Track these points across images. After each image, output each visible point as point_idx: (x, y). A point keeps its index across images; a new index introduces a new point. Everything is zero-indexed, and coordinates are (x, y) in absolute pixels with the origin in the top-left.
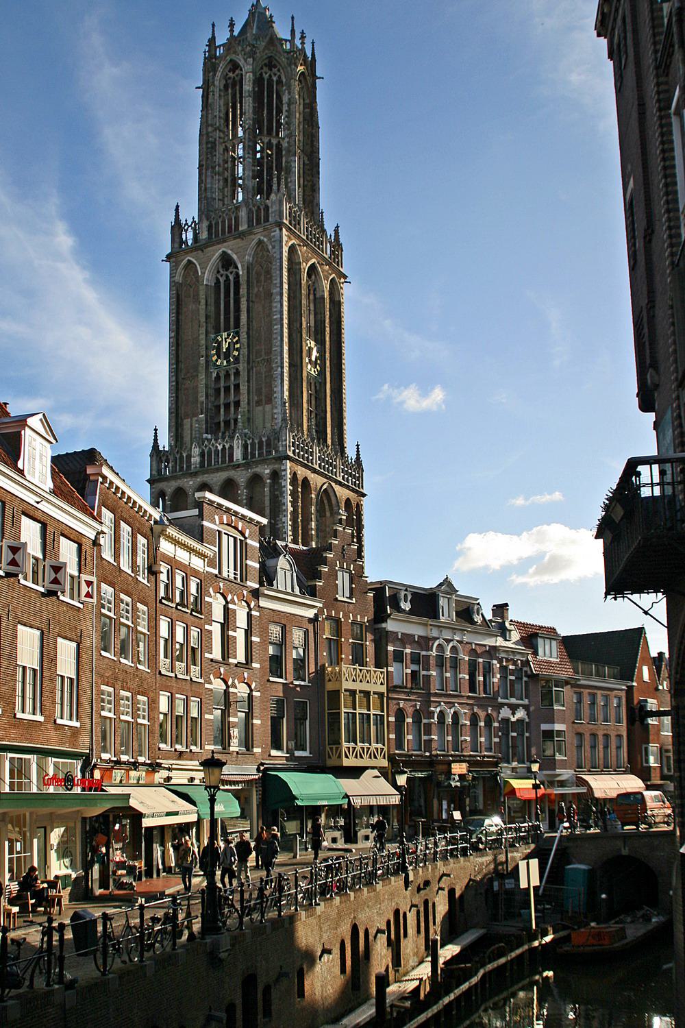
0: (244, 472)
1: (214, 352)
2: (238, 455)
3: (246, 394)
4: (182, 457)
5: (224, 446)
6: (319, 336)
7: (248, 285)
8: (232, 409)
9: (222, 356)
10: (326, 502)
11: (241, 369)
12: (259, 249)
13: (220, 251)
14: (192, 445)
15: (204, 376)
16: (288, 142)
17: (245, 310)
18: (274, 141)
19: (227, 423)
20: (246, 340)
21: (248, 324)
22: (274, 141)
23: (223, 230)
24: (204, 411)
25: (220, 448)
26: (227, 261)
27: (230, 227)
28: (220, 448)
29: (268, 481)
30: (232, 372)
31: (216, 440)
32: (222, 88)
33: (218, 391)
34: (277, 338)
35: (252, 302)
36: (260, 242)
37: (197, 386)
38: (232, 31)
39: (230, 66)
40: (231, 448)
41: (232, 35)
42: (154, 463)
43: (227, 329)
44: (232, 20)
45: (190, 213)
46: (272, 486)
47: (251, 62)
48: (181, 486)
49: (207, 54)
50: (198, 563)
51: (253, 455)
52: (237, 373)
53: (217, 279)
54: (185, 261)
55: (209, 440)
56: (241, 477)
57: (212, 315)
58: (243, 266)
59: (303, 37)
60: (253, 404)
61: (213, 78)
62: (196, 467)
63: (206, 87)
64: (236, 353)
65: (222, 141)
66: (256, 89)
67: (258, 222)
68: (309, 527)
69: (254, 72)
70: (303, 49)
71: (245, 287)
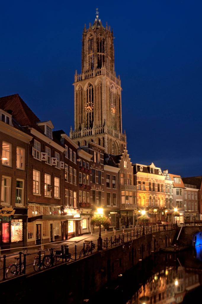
2: (93, 133)
13: (88, 83)
28: (89, 131)
29: (102, 140)
40: (91, 132)
58: (94, 86)
71: (95, 91)
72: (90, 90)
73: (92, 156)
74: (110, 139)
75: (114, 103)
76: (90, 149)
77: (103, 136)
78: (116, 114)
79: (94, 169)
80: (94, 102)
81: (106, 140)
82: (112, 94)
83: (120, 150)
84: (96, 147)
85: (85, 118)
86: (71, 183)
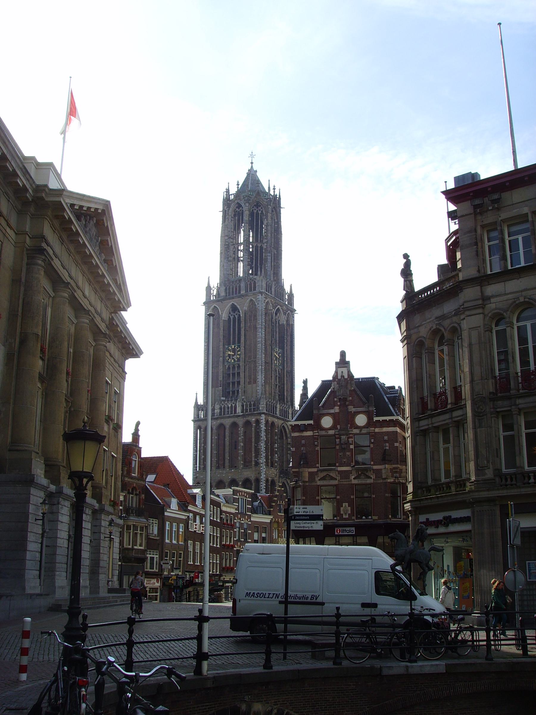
0: (242, 419)
2: (239, 410)
3: (243, 379)
5: (232, 405)
7: (245, 322)
8: (236, 385)
10: (283, 432)
11: (241, 365)
12: (251, 303)
13: (231, 303)
14: (215, 403)
15: (222, 367)
16: (266, 246)
17: (243, 335)
18: (259, 245)
19: (233, 392)
20: (244, 351)
21: (245, 343)
22: (259, 245)
24: (222, 385)
25: (230, 406)
26: (234, 308)
27: (236, 289)
28: (230, 406)
29: (254, 424)
30: (236, 366)
31: (228, 401)
32: (233, 216)
33: (229, 375)
34: (259, 351)
35: (247, 331)
36: (251, 300)
37: (218, 372)
38: (238, 187)
41: (238, 190)
42: (195, 411)
44: (238, 182)
45: (215, 282)
46: (256, 427)
47: (248, 205)
49: (225, 196)
50: (233, 511)
51: (247, 410)
52: (239, 367)
53: (229, 317)
54: (213, 306)
55: (224, 401)
56: (241, 422)
59: (274, 189)
60: (247, 383)
61: (228, 211)
62: (217, 415)
63: (225, 213)
65: (232, 243)
66: (250, 219)
67: (251, 290)
68: (275, 447)
69: (249, 211)
70: (274, 193)
71: (243, 323)
72: (234, 317)
73: (238, 504)
74: (270, 423)
76: (234, 496)
79: (239, 521)
80: (242, 344)
81: (263, 427)
82: (277, 325)
83: (290, 444)
84: (242, 492)
86: (215, 546)
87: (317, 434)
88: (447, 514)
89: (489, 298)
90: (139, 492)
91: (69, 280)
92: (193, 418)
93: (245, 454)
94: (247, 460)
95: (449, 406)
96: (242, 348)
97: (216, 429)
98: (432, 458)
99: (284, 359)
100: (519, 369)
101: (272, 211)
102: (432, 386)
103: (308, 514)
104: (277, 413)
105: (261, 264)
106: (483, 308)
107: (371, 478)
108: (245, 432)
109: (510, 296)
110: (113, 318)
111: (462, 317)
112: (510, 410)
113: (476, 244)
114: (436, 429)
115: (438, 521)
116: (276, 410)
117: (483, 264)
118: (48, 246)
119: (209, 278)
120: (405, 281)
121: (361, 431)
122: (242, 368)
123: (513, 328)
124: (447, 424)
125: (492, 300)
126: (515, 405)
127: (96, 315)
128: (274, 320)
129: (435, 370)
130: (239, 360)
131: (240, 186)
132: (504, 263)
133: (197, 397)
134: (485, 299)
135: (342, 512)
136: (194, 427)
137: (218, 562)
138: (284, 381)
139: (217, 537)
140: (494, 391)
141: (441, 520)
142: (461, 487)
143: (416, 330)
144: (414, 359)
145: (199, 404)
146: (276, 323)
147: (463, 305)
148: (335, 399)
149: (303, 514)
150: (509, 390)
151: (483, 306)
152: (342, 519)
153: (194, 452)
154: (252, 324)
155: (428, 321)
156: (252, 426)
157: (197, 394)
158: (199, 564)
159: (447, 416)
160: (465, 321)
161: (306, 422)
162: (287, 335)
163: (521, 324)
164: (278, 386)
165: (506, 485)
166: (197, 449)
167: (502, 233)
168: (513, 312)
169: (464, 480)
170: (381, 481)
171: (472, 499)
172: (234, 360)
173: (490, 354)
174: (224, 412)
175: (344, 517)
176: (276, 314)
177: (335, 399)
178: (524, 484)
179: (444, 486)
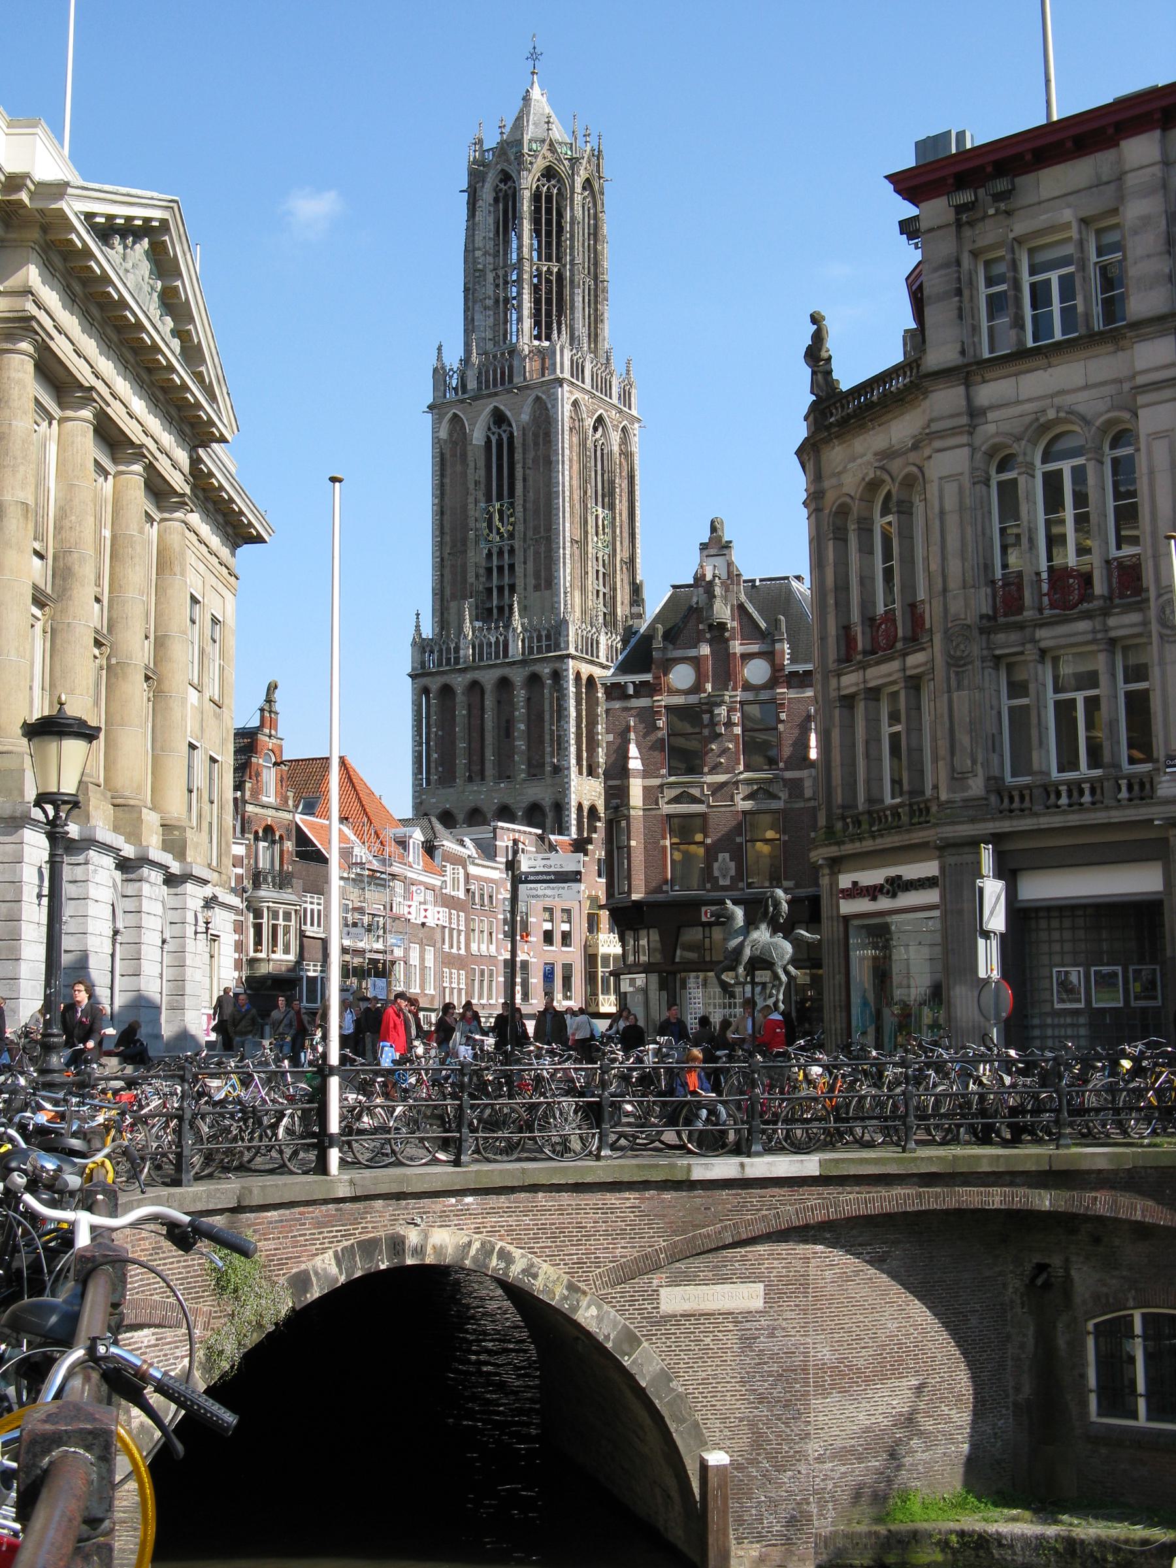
0: (521, 670)
1: (485, 524)
4: (448, 649)
6: (606, 500)
9: (494, 531)
11: (516, 547)
13: (491, 406)
19: (501, 609)
23: (495, 379)
25: (493, 640)
26: (499, 418)
27: (503, 374)
28: (493, 640)
29: (549, 682)
30: (506, 549)
33: (489, 570)
36: (538, 398)
37: (465, 564)
39: (500, 176)
43: (500, 498)
45: (453, 358)
48: (448, 682)
52: (512, 551)
53: (488, 438)
54: (450, 415)
56: (518, 676)
57: (483, 480)
60: (530, 588)
64: (510, 528)
74: (584, 677)
75: (603, 496)
77: (557, 665)
78: (614, 550)
80: (519, 502)
85: (477, 576)
86: (454, 951)
87: (663, 703)
88: (892, 871)
89: (983, 412)
90: (281, 837)
91: (91, 380)
92: (409, 670)
93: (529, 748)
94: (534, 762)
95: (899, 645)
96: (519, 509)
97: (463, 693)
98: (867, 756)
99: (614, 532)
100: (1043, 565)
101: (584, 188)
102: (867, 602)
103: (552, 869)
104: (601, 654)
105: (559, 316)
106: (971, 434)
107: (780, 798)
108: (529, 699)
109: (1029, 407)
110: (200, 460)
111: (927, 452)
112: (1022, 653)
113: (959, 292)
114: (873, 694)
115: (875, 887)
116: (598, 647)
117: (973, 335)
118: (40, 308)
119: (440, 349)
120: (814, 373)
121: (757, 695)
122: (519, 553)
123: (1033, 476)
124: (894, 683)
125: (991, 416)
126: (1033, 641)
127: (158, 454)
128: (590, 444)
129: (872, 566)
130: (511, 535)
131: (507, 130)
132: (1018, 335)
133: (418, 622)
134: (975, 414)
135: (716, 873)
136: (414, 689)
137: (463, 986)
138: (615, 583)
139: (459, 931)
140: (990, 613)
141: (882, 885)
142: (921, 815)
143: (834, 481)
144: (831, 543)
145: (424, 636)
146: (596, 451)
147: (928, 426)
148: (701, 627)
149: (542, 869)
150: (1020, 609)
151: (971, 430)
152: (717, 887)
153: (414, 746)
154: (540, 453)
155: (859, 461)
156: (542, 685)
157: (418, 615)
158: (418, 991)
159: (895, 665)
160: (932, 461)
161: (638, 678)
162: (621, 476)
163: (1052, 466)
164: (601, 595)
165: (1011, 811)
166: (421, 738)
167: (1014, 266)
168: (1034, 443)
169: (929, 800)
170: (801, 805)
171: (941, 839)
172: (502, 537)
173: (984, 534)
174: (481, 654)
175: (721, 882)
176: (595, 429)
177: (701, 627)
178: (1048, 808)
179: (888, 813)
